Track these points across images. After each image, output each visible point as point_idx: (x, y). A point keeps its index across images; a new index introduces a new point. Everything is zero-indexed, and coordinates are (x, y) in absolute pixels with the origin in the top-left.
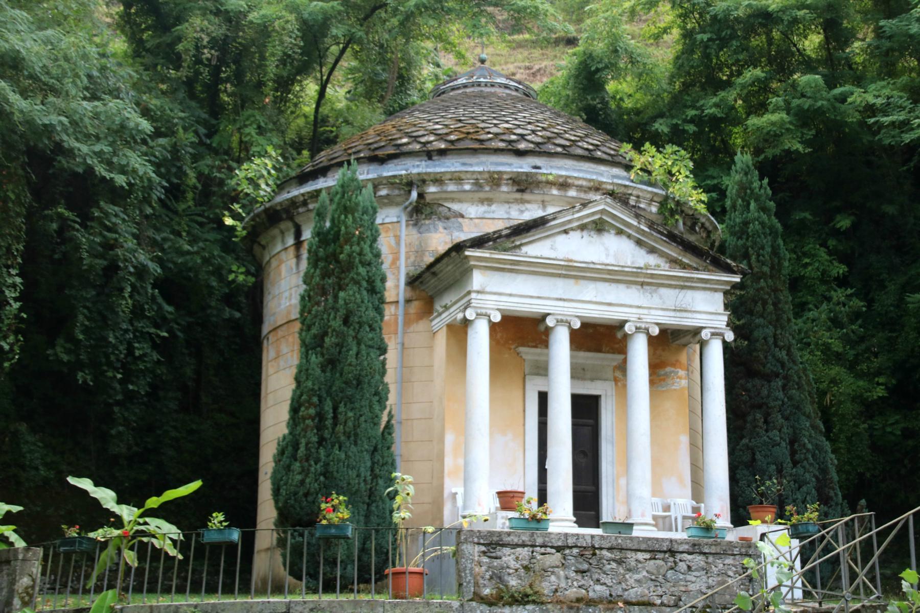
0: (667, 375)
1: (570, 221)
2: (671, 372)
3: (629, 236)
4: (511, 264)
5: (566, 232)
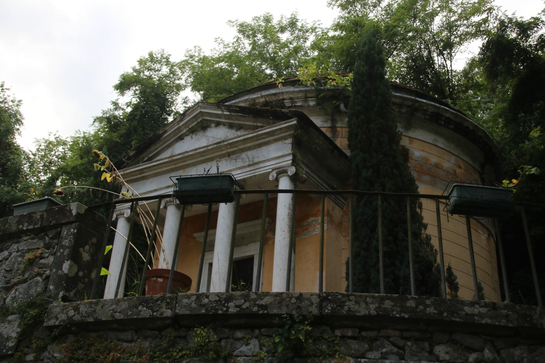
1: (179, 129)
2: (313, 221)
3: (224, 124)
4: (140, 174)
5: (181, 138)
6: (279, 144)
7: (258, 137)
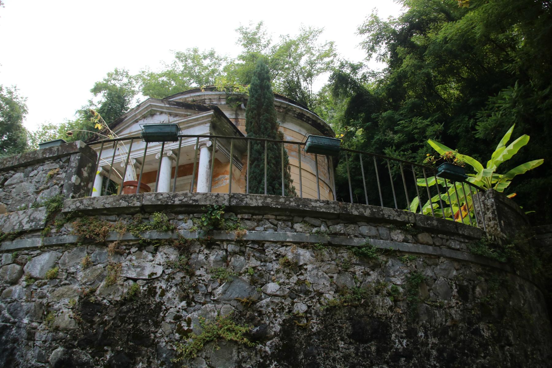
0: (219, 179)
3: (165, 113)
6: (202, 127)
7: (188, 122)
